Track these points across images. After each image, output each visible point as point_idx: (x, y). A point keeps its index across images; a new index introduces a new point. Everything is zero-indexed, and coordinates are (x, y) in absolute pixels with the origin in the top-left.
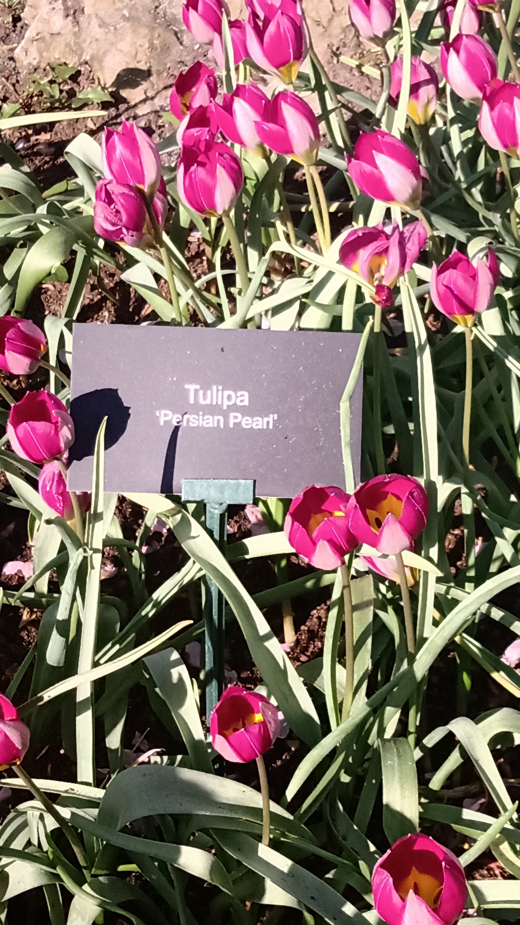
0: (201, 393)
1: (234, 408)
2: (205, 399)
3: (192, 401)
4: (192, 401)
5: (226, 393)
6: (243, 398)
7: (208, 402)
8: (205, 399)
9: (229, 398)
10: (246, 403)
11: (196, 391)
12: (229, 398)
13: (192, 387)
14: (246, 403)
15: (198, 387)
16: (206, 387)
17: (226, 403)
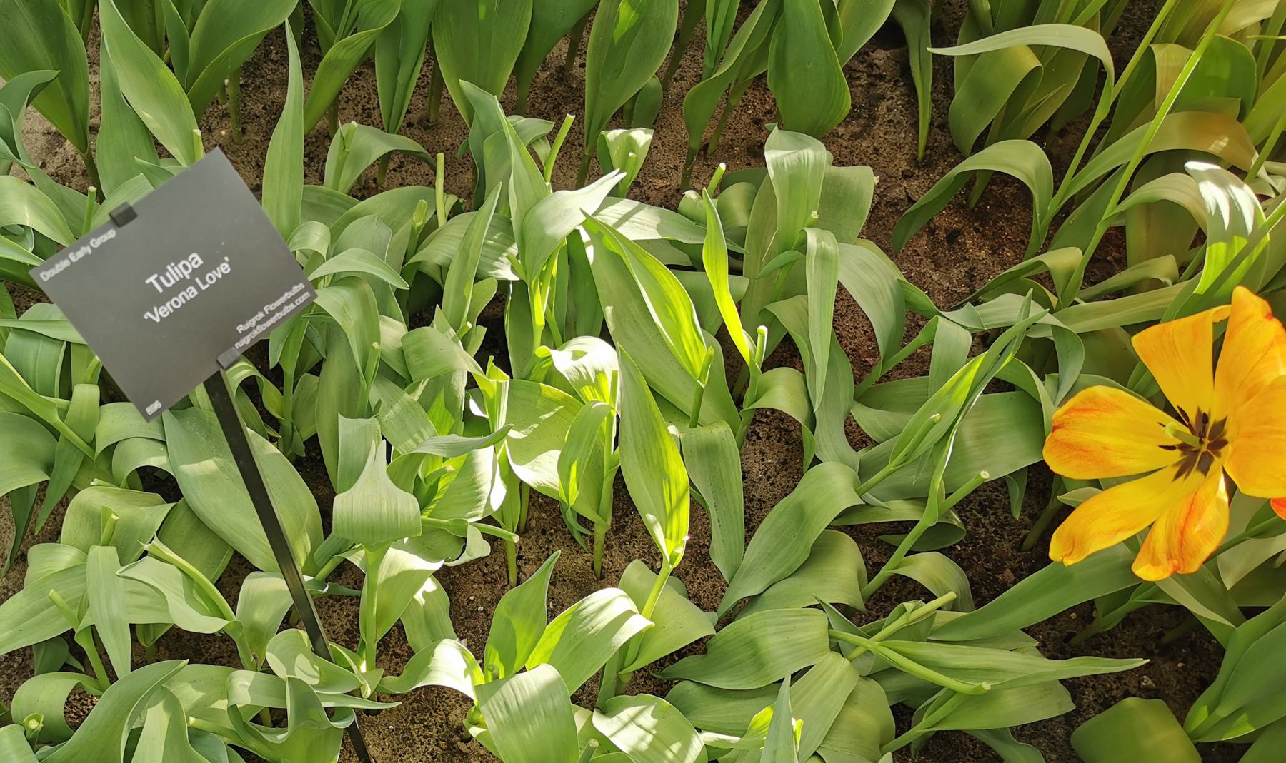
0: (162, 278)
1: (195, 273)
2: (168, 281)
3: (160, 290)
4: (160, 290)
5: (180, 265)
6: (196, 260)
7: (173, 282)
8: (168, 281)
9: (186, 267)
10: (201, 262)
11: (157, 279)
12: (186, 267)
13: (152, 279)
14: (201, 262)
15: (155, 276)
16: (163, 271)
17: (187, 273)
